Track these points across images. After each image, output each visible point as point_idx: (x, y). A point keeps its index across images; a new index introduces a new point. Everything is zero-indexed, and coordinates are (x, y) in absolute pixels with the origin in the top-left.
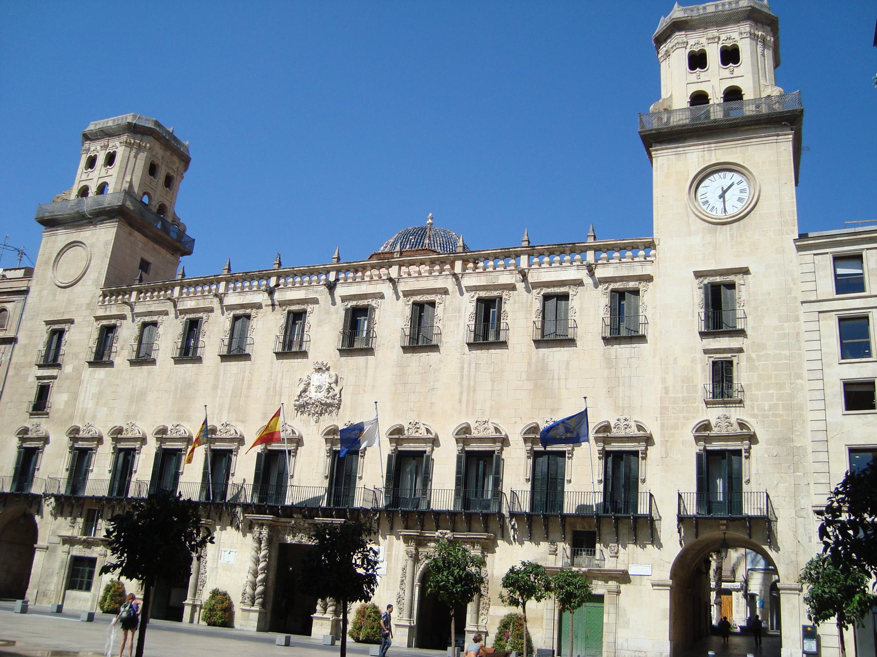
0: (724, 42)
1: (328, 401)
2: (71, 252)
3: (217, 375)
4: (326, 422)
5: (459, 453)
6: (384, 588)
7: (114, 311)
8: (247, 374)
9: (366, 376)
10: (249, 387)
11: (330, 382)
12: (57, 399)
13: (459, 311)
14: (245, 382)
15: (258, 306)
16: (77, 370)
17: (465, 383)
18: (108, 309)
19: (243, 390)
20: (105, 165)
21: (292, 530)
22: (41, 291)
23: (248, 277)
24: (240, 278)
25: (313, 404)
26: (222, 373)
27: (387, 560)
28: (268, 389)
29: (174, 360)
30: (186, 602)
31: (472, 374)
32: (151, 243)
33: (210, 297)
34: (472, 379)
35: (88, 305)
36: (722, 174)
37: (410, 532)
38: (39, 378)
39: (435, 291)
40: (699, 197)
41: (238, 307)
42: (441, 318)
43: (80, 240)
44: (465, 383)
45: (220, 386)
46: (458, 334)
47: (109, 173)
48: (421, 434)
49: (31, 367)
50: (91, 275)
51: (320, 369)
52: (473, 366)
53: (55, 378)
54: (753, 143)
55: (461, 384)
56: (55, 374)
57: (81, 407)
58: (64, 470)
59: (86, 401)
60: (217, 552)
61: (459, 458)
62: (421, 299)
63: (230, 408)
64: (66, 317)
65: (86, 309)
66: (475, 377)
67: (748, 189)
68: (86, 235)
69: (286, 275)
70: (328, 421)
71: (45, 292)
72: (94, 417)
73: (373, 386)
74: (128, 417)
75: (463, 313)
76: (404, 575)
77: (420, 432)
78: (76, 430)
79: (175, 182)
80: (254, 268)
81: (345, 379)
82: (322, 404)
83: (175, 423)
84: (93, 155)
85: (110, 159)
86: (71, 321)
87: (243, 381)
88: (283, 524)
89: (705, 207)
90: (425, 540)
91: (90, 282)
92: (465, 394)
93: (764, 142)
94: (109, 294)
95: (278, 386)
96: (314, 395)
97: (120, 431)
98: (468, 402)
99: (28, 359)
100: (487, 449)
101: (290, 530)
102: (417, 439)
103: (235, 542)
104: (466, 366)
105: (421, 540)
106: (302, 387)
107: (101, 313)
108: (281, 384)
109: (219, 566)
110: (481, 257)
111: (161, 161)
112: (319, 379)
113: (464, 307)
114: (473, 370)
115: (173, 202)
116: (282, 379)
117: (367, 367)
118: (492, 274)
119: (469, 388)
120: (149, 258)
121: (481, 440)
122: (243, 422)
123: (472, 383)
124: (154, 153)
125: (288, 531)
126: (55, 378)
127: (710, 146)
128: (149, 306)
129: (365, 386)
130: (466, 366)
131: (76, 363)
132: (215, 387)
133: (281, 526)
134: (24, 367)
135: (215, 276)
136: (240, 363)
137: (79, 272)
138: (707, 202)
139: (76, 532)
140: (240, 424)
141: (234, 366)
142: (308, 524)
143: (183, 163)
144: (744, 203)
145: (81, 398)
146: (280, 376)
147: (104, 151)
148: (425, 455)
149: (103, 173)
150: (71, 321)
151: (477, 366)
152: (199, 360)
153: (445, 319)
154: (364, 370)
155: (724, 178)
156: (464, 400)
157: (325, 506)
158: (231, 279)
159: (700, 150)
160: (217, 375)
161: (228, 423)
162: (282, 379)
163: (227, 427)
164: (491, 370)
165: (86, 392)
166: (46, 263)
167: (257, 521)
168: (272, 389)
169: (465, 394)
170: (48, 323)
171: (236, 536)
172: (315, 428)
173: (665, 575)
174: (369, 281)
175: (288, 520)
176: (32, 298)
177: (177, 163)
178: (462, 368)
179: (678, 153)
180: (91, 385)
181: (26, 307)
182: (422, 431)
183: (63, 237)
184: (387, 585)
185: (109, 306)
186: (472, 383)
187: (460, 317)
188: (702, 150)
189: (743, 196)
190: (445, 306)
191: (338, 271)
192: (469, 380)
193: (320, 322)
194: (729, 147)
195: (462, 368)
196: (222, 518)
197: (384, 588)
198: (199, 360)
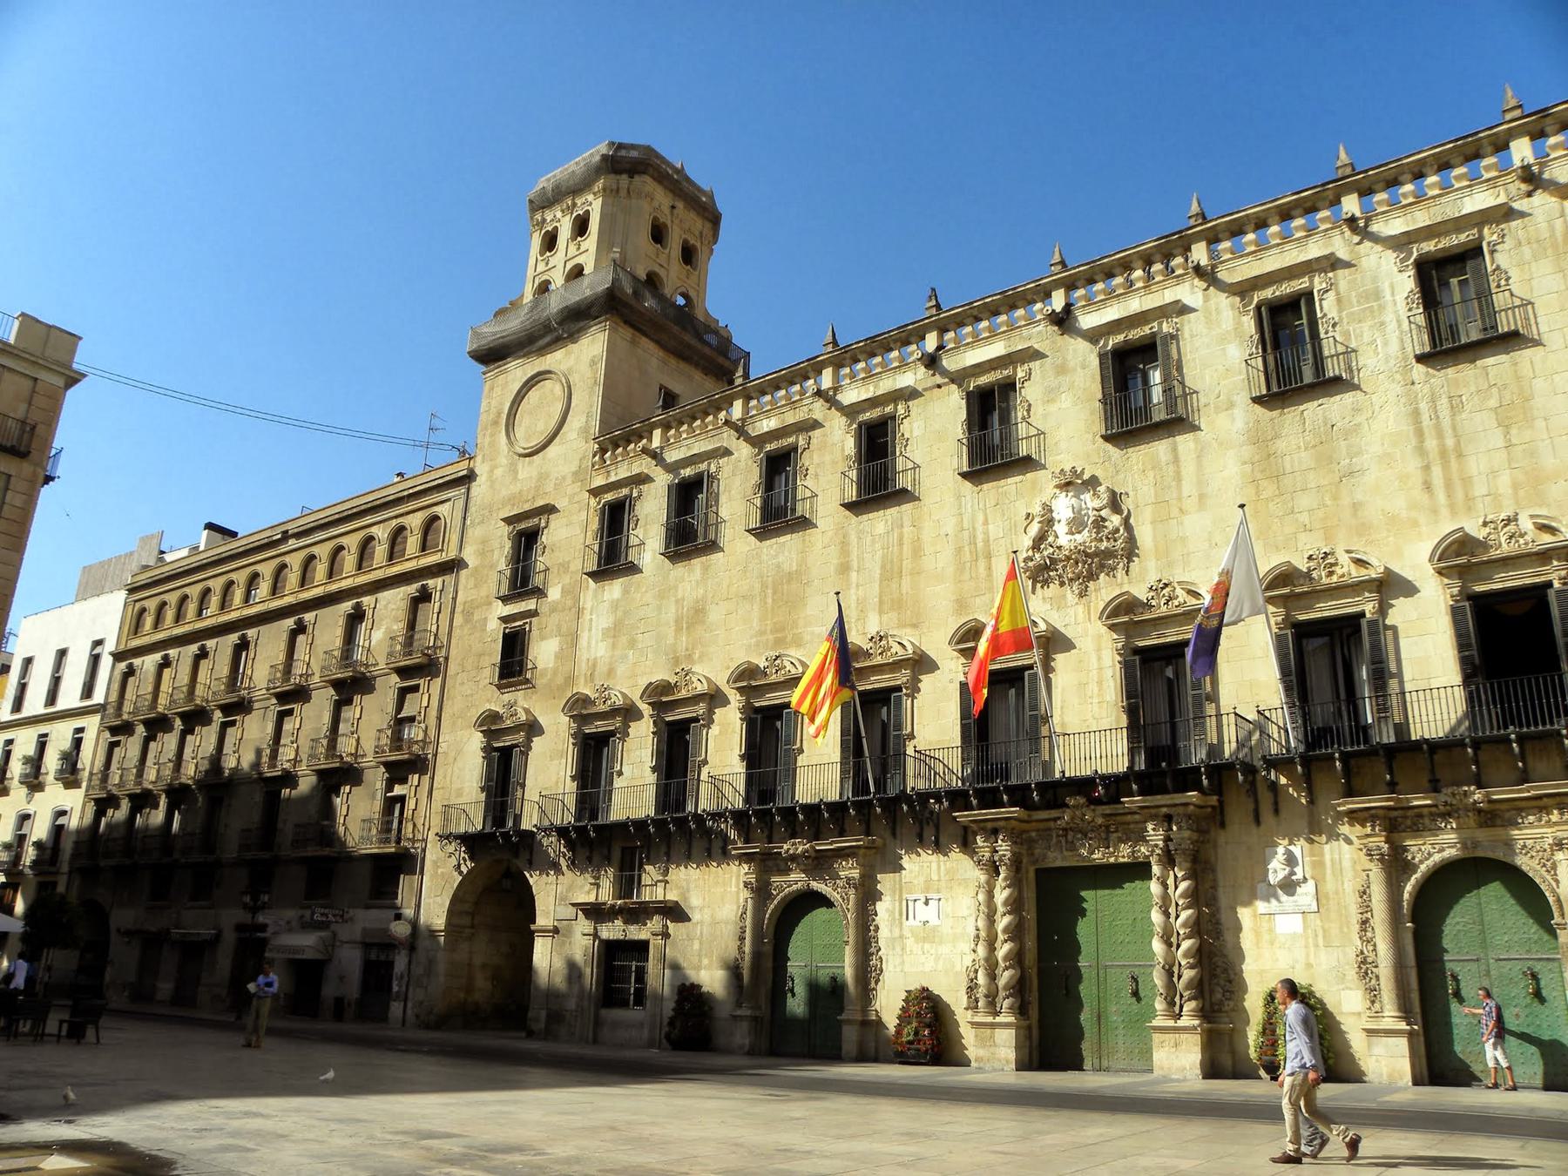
1: (1104, 545)
2: (533, 395)
3: (844, 546)
4: (1103, 591)
5: (1456, 601)
6: (1316, 946)
7: (622, 472)
8: (907, 530)
9: (1178, 477)
10: (917, 552)
11: (1096, 506)
12: (543, 652)
13: (1377, 295)
14: (905, 547)
15: (910, 394)
16: (573, 593)
17: (1431, 444)
18: (613, 474)
19: (905, 562)
20: (573, 238)
21: (1066, 836)
22: (492, 471)
23: (877, 346)
24: (861, 352)
25: (1068, 558)
26: (853, 538)
27: (1312, 878)
28: (959, 550)
29: (753, 535)
30: (843, 1017)
31: (1446, 422)
32: (673, 361)
33: (805, 402)
34: (1448, 433)
35: (575, 474)
37: (1370, 801)
38: (504, 619)
39: (1308, 268)
41: (866, 405)
42: (1336, 319)
43: (547, 368)
44: (1431, 444)
45: (855, 565)
46: (1386, 344)
47: (582, 249)
48: (1343, 576)
49: (490, 604)
50: (575, 422)
51: (1068, 484)
52: (1443, 403)
53: (533, 614)
55: (1421, 450)
56: (533, 607)
57: (584, 658)
58: (568, 779)
59: (594, 642)
60: (897, 904)
61: (1456, 612)
62: (1277, 293)
63: (881, 602)
64: (540, 503)
65: (573, 482)
66: (1454, 428)
68: (556, 360)
69: (958, 322)
70: (1106, 590)
71: (499, 472)
72: (611, 672)
73: (1202, 497)
74: (676, 661)
75: (1388, 297)
76: (1366, 907)
77: (1339, 570)
78: (585, 701)
79: (701, 255)
80: (887, 324)
81: (1131, 493)
82: (1087, 555)
83: (773, 654)
84: (550, 229)
85: (581, 227)
86: (550, 510)
87: (901, 544)
88: (1041, 826)
90: (1406, 817)
91: (573, 435)
92: (1437, 471)
94: (610, 447)
95: (980, 537)
96: (1064, 538)
97: (666, 688)
98: (1448, 485)
99: (483, 592)
100: (1528, 581)
101: (1058, 836)
102: (1335, 588)
103: (935, 877)
104: (1424, 406)
105: (1395, 819)
106: (1035, 528)
107: (599, 481)
108: (986, 533)
109: (906, 933)
110: (1404, 173)
111: (669, 217)
112: (1064, 507)
113: (1387, 285)
115: (701, 285)
116: (986, 522)
118: (1443, 200)
119: (1443, 453)
120: (676, 387)
121: (1507, 562)
122: (915, 626)
123: (1450, 442)
124: (656, 204)
125: (1054, 840)
126: (533, 614)
128: (689, 448)
129: (1180, 499)
130: (1424, 406)
131: (567, 580)
133: (1038, 830)
134: (478, 607)
135: (808, 360)
136: (889, 511)
137: (553, 423)
139: (606, 893)
140: (908, 630)
141: (880, 521)
142: (1104, 816)
143: (708, 225)
145: (583, 642)
146: (981, 517)
147: (568, 217)
148: (1364, 622)
149: (572, 249)
150: (550, 510)
151: (1456, 406)
152: (805, 523)
153: (1345, 321)
154: (1171, 468)
157: (1143, 767)
158: (843, 357)
160: (844, 546)
161: (882, 634)
162: (986, 522)
163: (883, 643)
164: (1493, 403)
165: (590, 630)
166: (496, 423)
167: (982, 825)
168: (967, 549)
169: (1437, 471)
170: (509, 521)
171: (934, 866)
172: (1080, 609)
174: (1145, 287)
175: (1054, 813)
176: (479, 489)
177: (698, 224)
178: (1416, 413)
180: (598, 616)
181: (472, 503)
182: (1345, 570)
183: (517, 371)
184: (1324, 937)
185: (613, 467)
186: (1450, 442)
187: (1382, 308)
190: (1338, 294)
191: (1070, 285)
192: (1440, 435)
193: (1051, 395)
196: (898, 832)
197: (1316, 946)
198: (805, 523)
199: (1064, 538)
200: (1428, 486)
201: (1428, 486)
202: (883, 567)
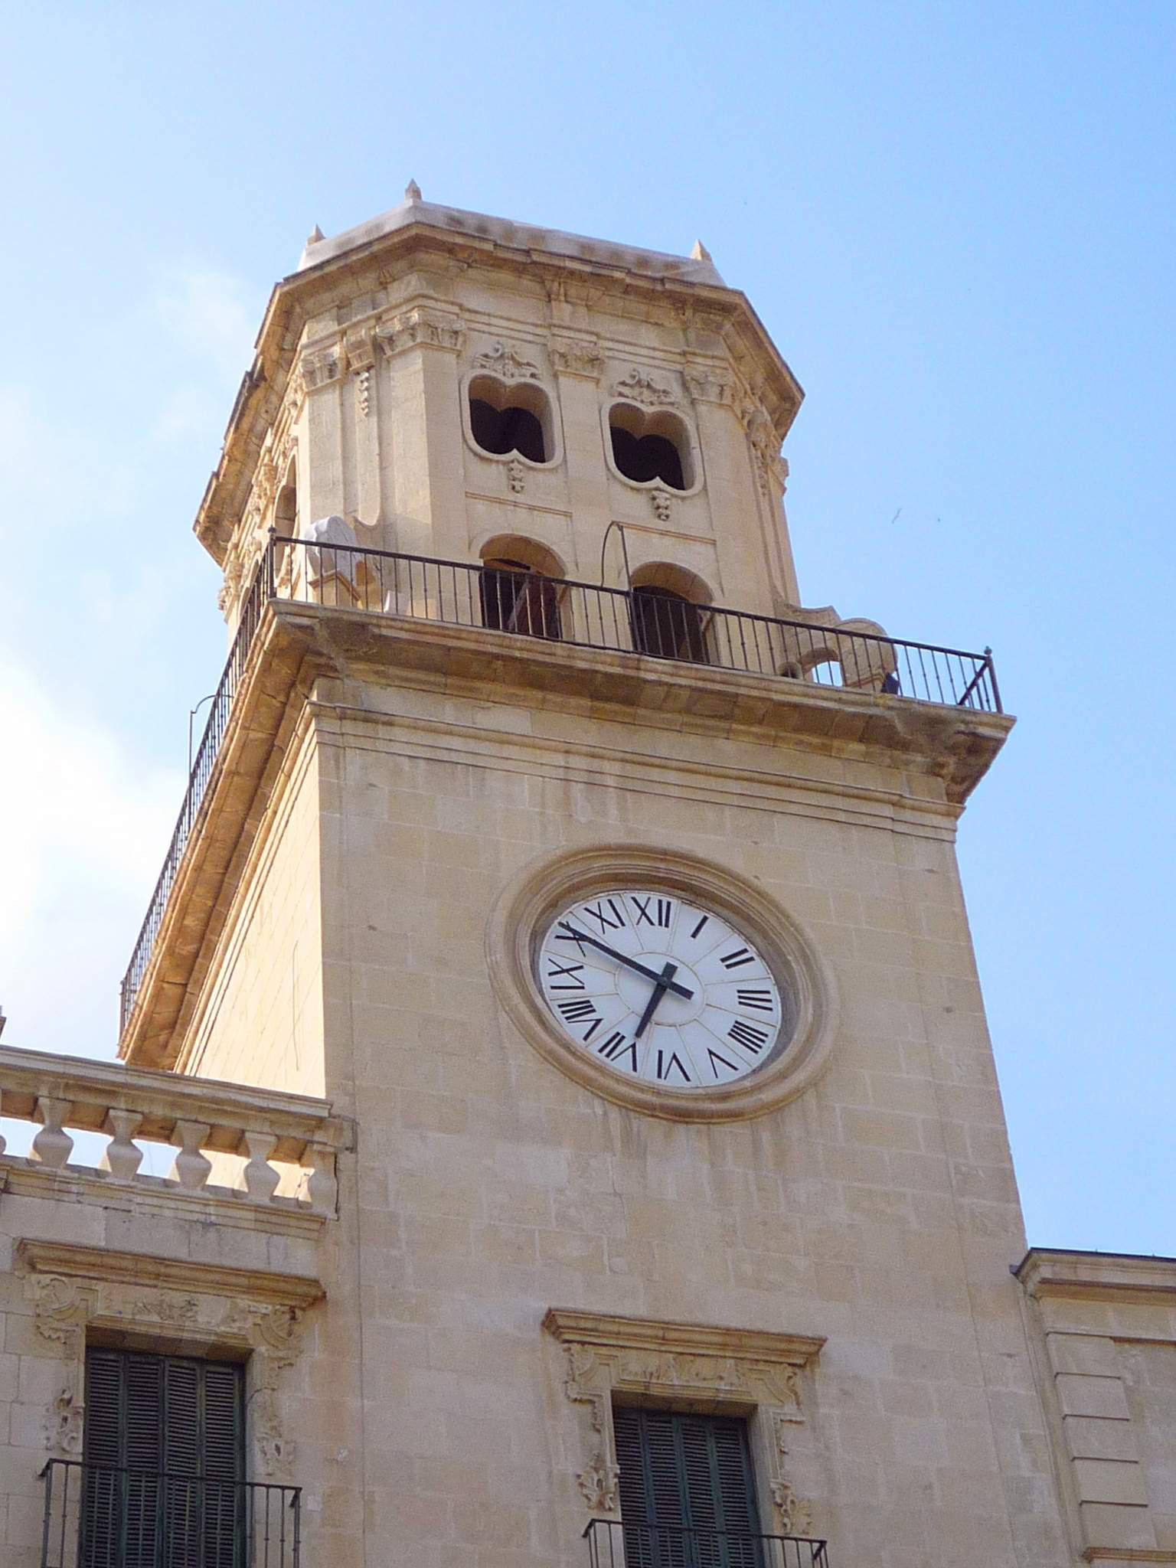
0: (626, 390)
36: (652, 899)
40: (547, 981)
54: (793, 809)
67: (775, 996)
89: (575, 1031)
93: (842, 817)
127: (596, 764)
138: (587, 1007)
144: (765, 1052)
155: (665, 920)
159: (546, 771)
179: (444, 756)
188: (561, 773)
189: (753, 1017)
194: (686, 793)
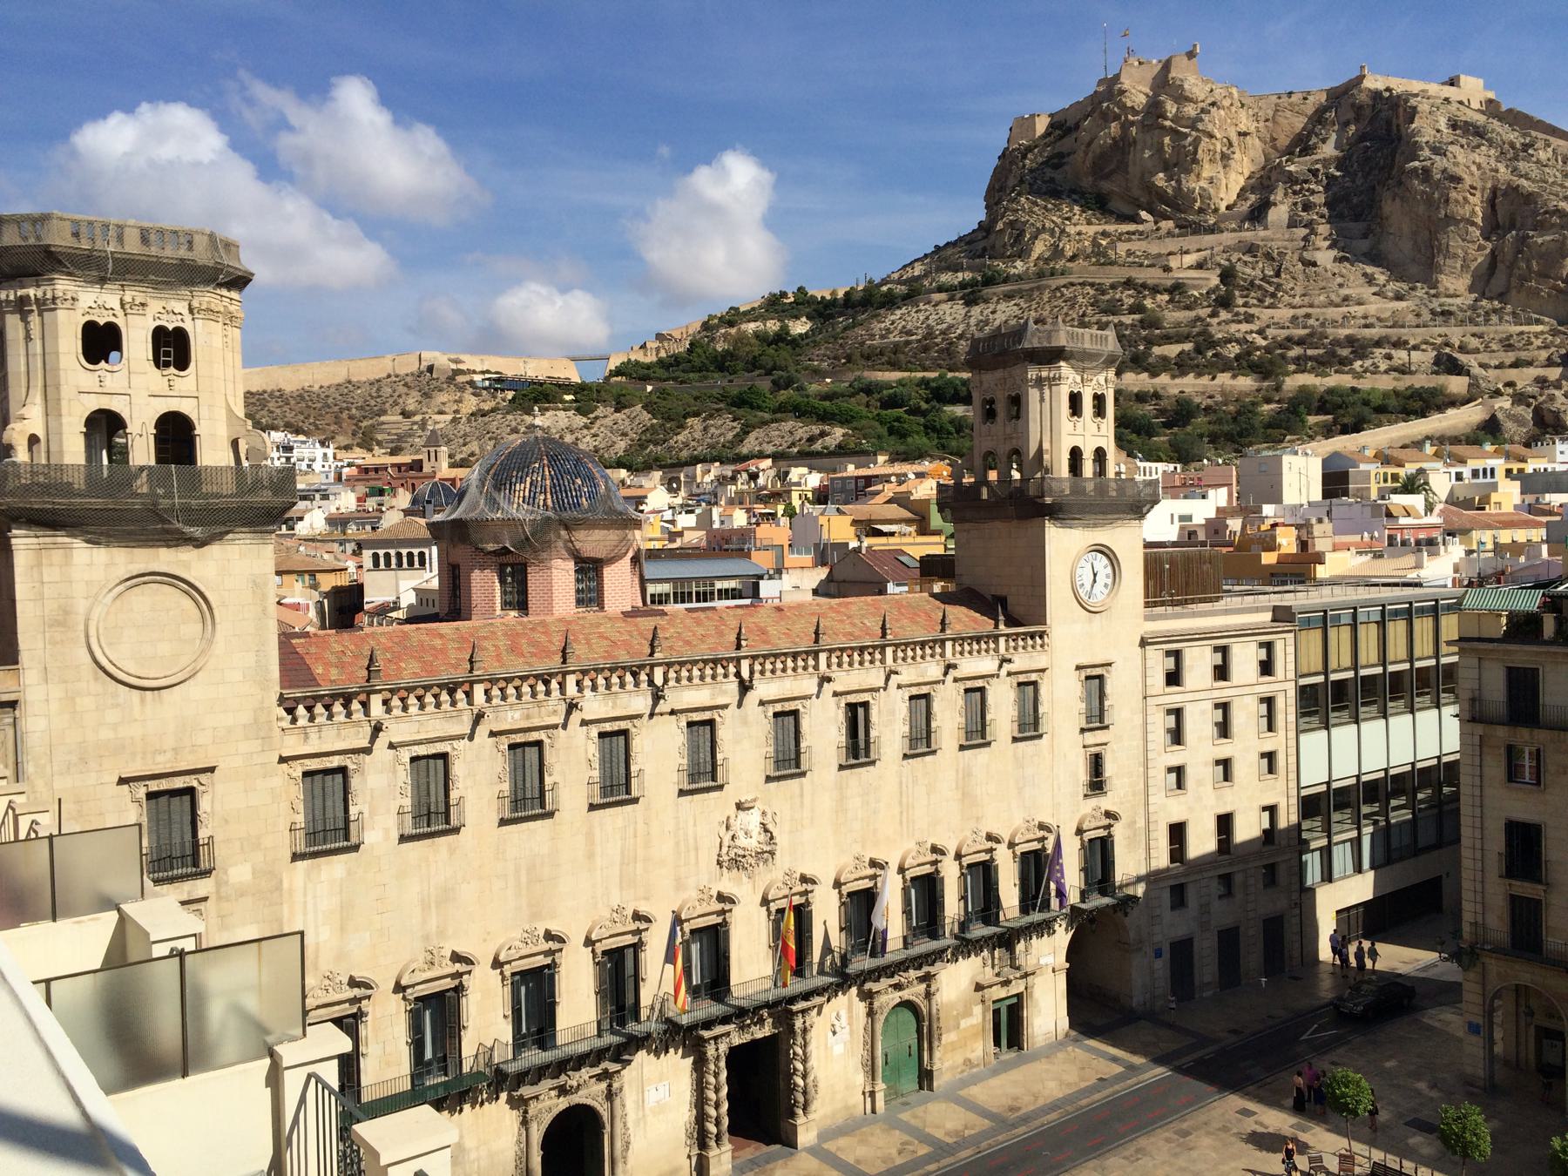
3: (590, 837)
28: (677, 844)
44: (904, 800)
55: (901, 803)
107: (293, 746)
114: (910, 785)
116: (695, 825)
117: (802, 795)
122: (647, 899)
132: (591, 856)
146: (691, 823)
156: (904, 820)
160: (590, 837)
162: (695, 825)
165: (305, 914)
173: (1061, 960)
178: (901, 783)
195: (901, 783)
199: (742, 841)
200: (901, 823)
201: (901, 823)
202: (622, 853)
